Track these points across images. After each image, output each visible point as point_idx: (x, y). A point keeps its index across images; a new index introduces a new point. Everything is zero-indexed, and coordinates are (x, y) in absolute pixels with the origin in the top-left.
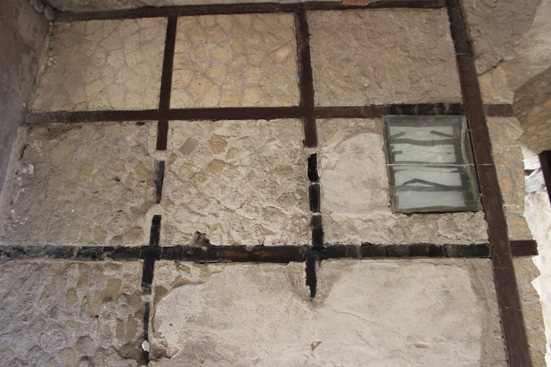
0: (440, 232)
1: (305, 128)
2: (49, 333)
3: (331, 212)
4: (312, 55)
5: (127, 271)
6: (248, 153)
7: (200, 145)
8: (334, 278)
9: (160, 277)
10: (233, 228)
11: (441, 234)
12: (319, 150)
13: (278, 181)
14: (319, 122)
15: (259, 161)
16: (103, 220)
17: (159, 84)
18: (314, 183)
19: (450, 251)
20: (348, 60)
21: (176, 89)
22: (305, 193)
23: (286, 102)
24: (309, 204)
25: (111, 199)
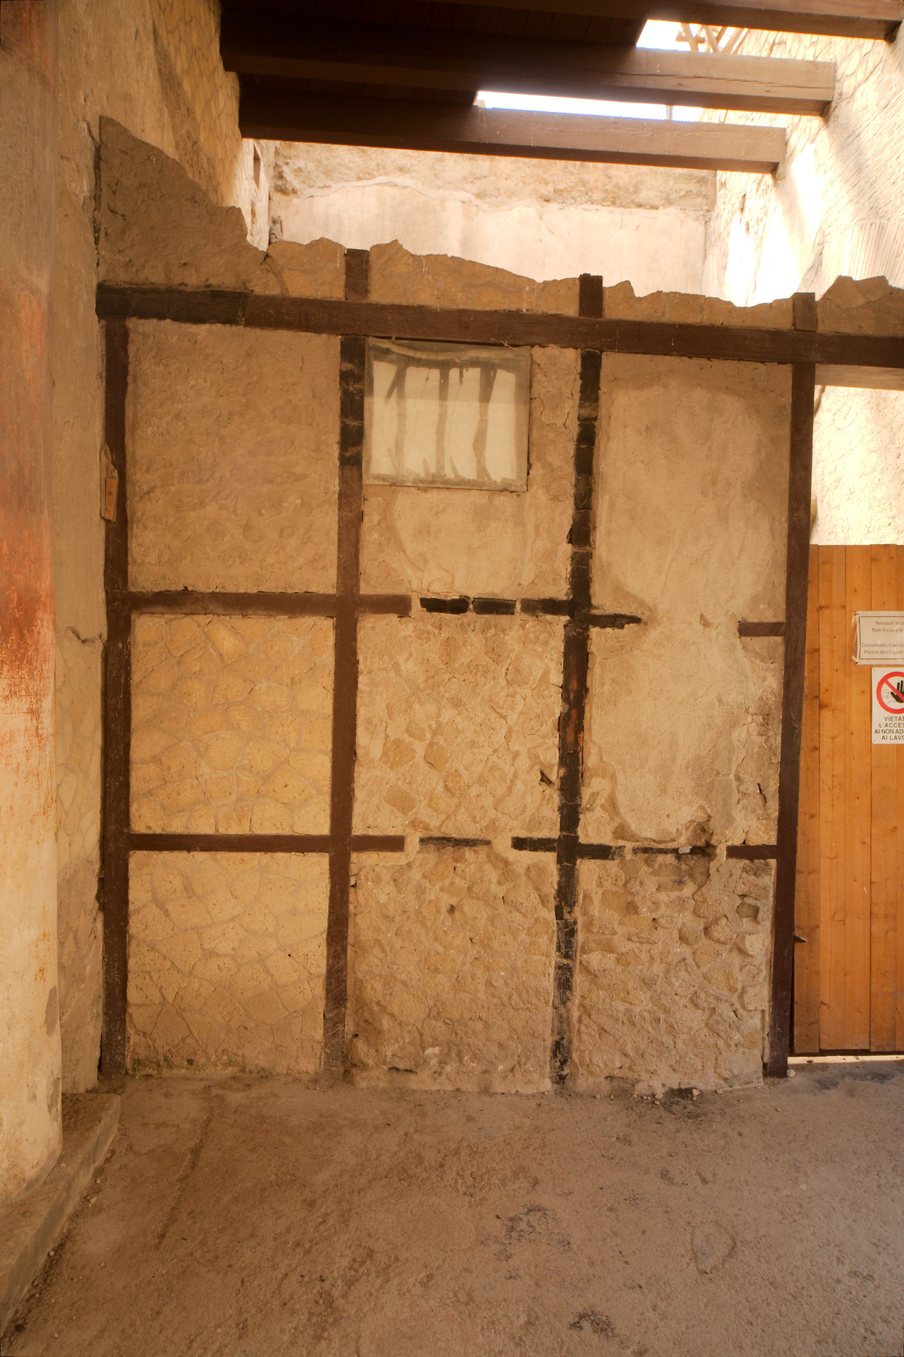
0: (560, 422)
1: (375, 613)
2: (677, 984)
3: (520, 584)
4: (231, 589)
5: (594, 883)
6: (417, 706)
7: (399, 782)
8: (619, 590)
9: (603, 835)
10: (538, 731)
11: (563, 422)
12: (415, 594)
13: (466, 661)
14: (365, 589)
15: (433, 688)
16: (519, 924)
17: (280, 856)
18: (471, 606)
19: (588, 412)
20: (247, 527)
21: (291, 827)
22: (486, 621)
23: (326, 641)
24: (504, 616)
25: (486, 916)
